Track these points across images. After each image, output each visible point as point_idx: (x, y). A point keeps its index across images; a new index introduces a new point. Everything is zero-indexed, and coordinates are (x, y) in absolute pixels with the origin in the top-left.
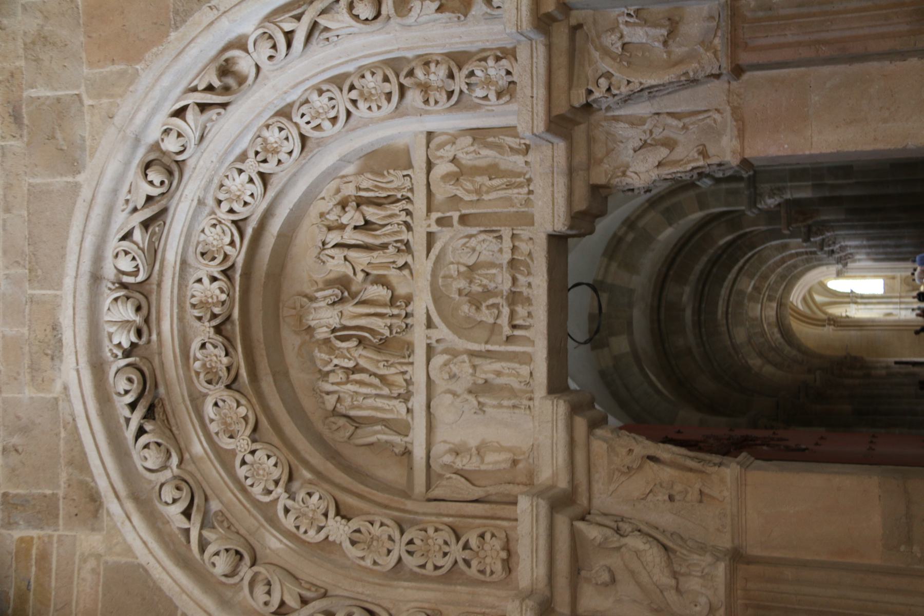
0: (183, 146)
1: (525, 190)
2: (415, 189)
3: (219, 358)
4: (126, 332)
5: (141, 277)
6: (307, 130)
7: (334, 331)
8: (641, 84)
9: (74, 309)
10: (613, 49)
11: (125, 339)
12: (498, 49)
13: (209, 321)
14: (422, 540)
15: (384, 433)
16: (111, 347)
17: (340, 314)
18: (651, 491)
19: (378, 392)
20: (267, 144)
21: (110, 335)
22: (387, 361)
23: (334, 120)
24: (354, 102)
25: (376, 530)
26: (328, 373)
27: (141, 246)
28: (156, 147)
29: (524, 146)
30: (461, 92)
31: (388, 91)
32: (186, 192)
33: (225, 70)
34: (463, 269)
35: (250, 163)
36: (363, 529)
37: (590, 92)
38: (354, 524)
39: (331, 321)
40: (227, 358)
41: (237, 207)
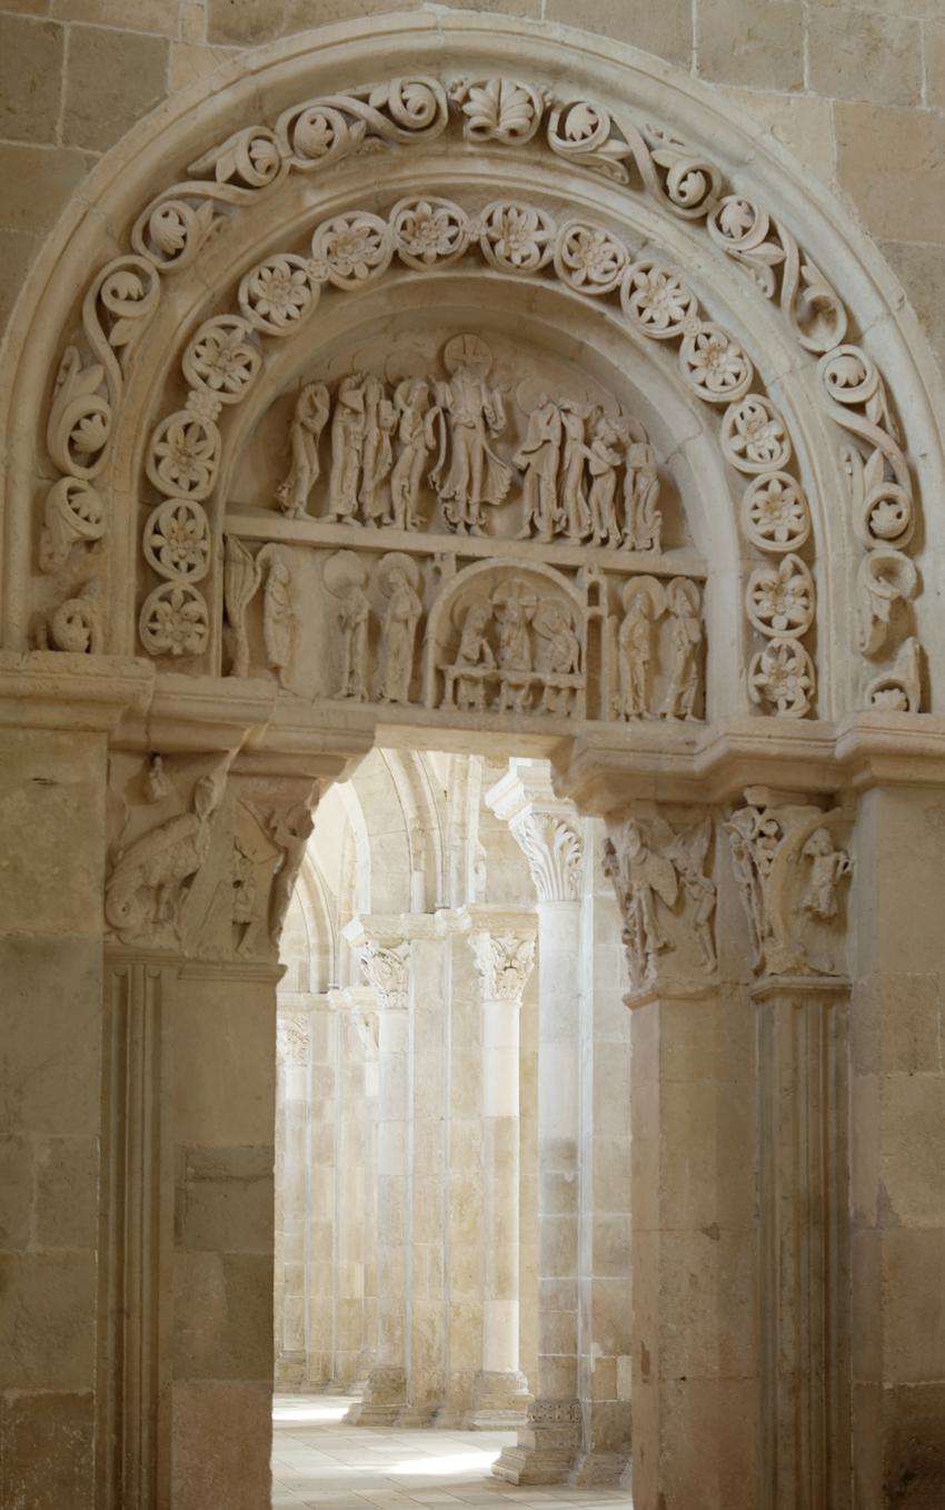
0: (729, 231)
1: (630, 710)
2: (636, 554)
3: (433, 243)
4: (486, 111)
5: (554, 139)
6: (732, 414)
7: (446, 411)
8: (767, 876)
9: (520, 34)
10: (810, 843)
11: (478, 108)
12: (816, 694)
13: (488, 236)
14: (192, 532)
15: (310, 478)
16: (467, 84)
17: (471, 425)
18: (244, 856)
19: (368, 473)
20: (718, 351)
21: (482, 86)
22: (409, 492)
23: (743, 454)
24: (765, 487)
25: (202, 463)
26: (390, 397)
27: (601, 149)
28: (727, 190)
29: (683, 712)
30: (769, 638)
31: (777, 535)
32: (662, 223)
33: (819, 310)
34: (529, 613)
35: (695, 325)
36: (203, 444)
37: (761, 810)
38: (212, 433)
39: (461, 411)
40: (435, 256)
41: (638, 296)
